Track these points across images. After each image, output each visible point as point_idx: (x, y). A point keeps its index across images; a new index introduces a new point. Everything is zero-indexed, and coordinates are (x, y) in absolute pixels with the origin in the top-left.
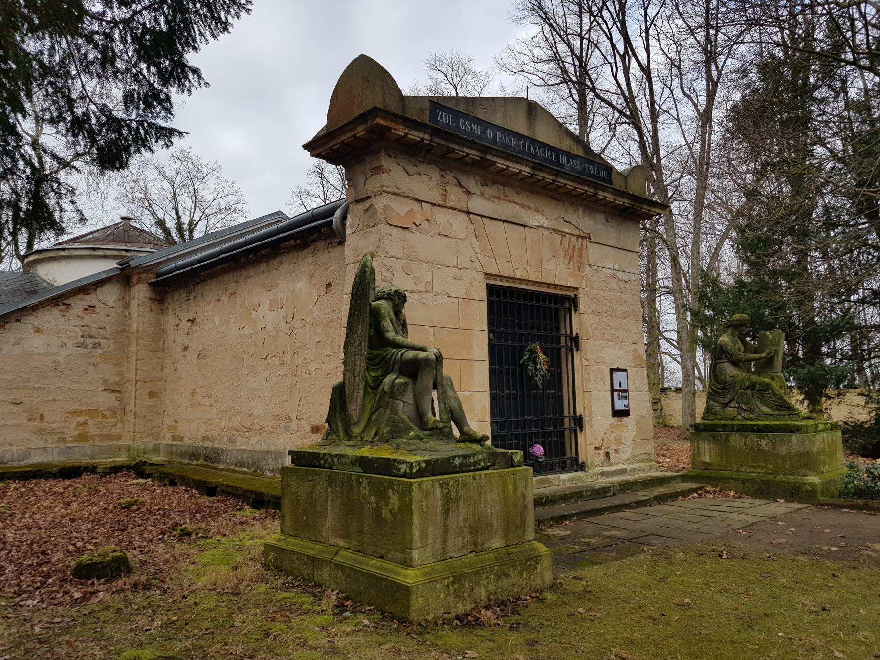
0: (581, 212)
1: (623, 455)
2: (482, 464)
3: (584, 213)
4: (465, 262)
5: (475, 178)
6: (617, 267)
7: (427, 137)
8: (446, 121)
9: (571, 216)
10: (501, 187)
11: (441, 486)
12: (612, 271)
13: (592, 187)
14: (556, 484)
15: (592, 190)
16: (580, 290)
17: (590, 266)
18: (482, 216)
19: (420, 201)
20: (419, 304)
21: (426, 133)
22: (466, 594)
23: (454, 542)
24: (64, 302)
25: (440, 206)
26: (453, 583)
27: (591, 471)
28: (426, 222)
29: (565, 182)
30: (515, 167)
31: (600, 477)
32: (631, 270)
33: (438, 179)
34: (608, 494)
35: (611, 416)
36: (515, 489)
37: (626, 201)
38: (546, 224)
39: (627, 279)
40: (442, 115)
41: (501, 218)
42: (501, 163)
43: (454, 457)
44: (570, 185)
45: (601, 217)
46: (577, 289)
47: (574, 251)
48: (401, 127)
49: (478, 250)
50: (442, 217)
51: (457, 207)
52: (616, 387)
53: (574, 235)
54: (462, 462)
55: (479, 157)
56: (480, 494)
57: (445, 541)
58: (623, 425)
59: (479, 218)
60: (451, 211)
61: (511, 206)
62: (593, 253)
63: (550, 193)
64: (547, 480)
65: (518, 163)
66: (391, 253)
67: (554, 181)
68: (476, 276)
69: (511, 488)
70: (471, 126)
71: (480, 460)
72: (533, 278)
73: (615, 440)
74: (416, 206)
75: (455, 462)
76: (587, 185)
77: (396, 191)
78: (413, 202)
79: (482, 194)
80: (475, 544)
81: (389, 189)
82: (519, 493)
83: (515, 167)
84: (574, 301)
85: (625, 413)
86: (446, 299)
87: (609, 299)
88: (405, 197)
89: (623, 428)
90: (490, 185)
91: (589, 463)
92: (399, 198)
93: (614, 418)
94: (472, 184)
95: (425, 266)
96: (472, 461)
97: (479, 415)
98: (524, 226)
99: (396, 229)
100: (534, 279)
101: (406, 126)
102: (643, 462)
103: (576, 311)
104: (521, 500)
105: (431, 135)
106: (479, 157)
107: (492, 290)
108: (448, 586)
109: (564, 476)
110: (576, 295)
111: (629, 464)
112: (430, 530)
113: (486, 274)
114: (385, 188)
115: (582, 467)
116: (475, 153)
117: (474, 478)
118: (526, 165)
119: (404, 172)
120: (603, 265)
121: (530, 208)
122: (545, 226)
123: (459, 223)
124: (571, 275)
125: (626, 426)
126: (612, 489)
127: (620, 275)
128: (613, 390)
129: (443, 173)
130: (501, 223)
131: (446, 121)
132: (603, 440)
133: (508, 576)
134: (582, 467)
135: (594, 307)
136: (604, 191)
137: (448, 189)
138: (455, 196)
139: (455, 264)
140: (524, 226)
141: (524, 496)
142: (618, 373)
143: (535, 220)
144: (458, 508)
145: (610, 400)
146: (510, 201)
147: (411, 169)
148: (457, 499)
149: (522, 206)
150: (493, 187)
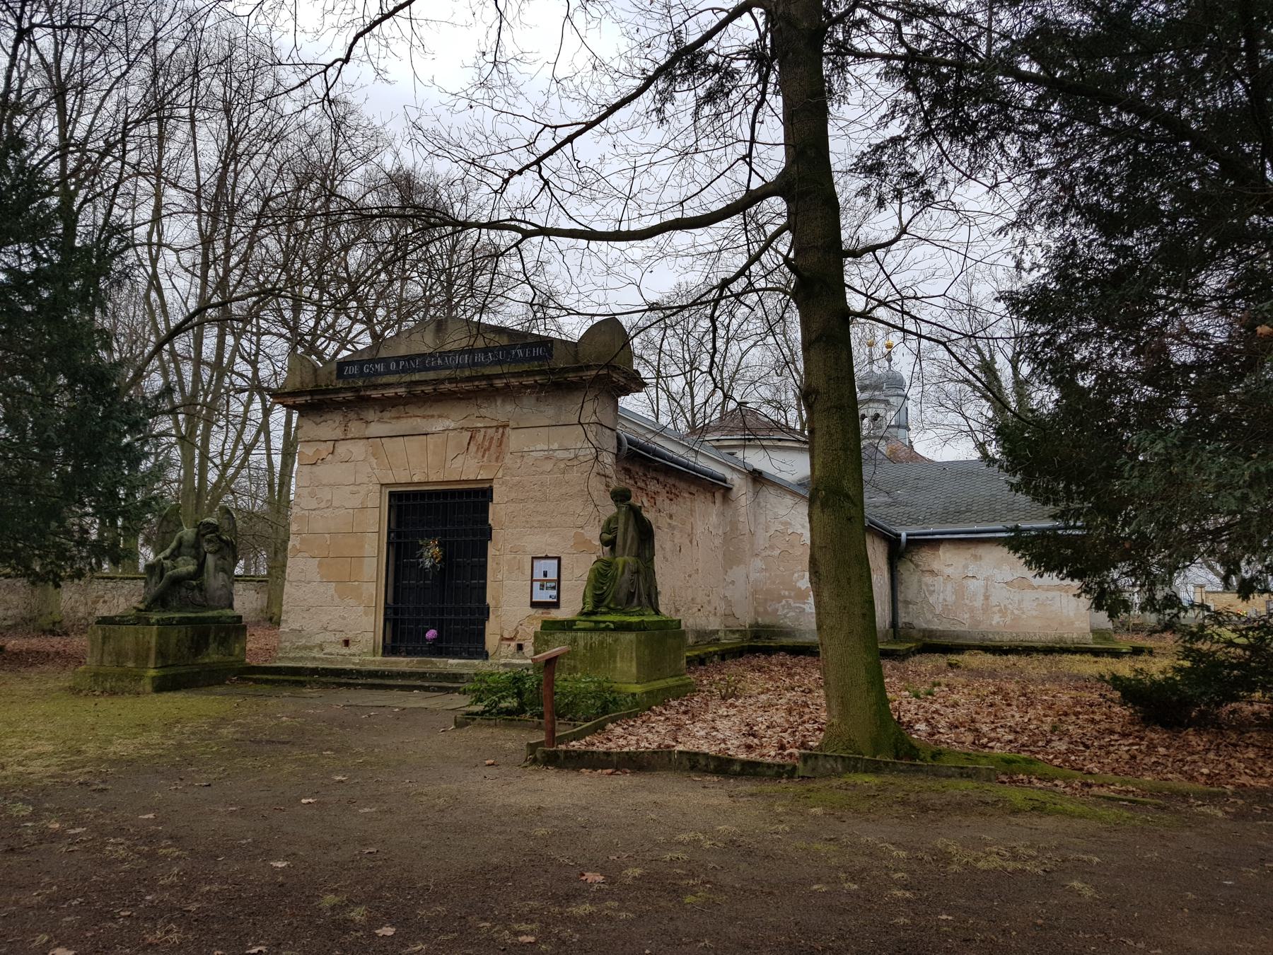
3: (503, 401)
6: (556, 446)
7: (308, 398)
23: (107, 659)
27: (490, 661)
37: (537, 378)
38: (452, 425)
45: (528, 401)
49: (375, 466)
50: (342, 448)
52: (538, 575)
61: (410, 420)
64: (432, 662)
72: (433, 478)
74: (322, 446)
86: (343, 511)
91: (490, 653)
94: (371, 415)
95: (327, 489)
107: (391, 494)
109: (451, 661)
116: (349, 394)
121: (432, 416)
123: (357, 450)
127: (560, 454)
128: (532, 581)
132: (517, 632)
134: (484, 655)
135: (513, 495)
138: (355, 428)
142: (543, 561)
143: (439, 425)
147: (318, 420)
148: (109, 637)
149: (424, 417)
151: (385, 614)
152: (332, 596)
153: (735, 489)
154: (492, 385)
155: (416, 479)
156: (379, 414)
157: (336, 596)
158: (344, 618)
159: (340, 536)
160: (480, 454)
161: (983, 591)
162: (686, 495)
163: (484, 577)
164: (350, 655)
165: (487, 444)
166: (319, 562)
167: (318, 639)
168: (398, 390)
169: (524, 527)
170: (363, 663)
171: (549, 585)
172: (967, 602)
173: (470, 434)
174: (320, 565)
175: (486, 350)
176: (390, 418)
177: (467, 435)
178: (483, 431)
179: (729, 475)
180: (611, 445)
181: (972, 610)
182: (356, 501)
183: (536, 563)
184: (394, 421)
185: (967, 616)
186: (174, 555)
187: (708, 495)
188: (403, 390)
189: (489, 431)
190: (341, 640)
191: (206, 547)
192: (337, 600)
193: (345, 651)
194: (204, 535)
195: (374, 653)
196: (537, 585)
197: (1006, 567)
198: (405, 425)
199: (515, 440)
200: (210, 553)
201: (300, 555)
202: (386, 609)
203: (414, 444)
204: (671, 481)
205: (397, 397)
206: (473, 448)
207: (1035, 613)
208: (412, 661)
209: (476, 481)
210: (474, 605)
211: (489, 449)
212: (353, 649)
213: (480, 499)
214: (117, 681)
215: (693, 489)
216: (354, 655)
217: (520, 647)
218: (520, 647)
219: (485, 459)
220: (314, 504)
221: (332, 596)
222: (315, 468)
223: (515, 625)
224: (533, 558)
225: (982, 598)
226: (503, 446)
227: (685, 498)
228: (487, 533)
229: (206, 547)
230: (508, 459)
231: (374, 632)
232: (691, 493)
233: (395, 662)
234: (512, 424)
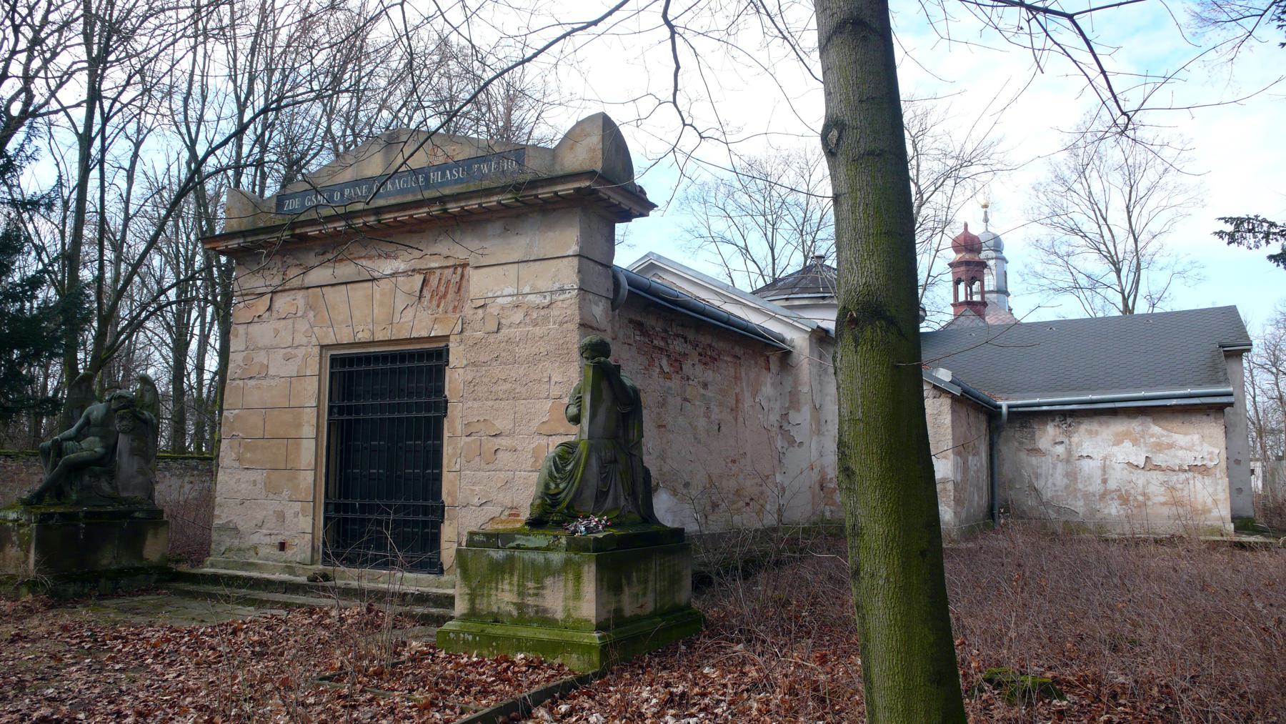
4: (300, 339)
6: (527, 290)
7: (241, 241)
16: (451, 337)
18: (321, 286)
29: (392, 215)
39: (547, 301)
46: (448, 336)
50: (282, 302)
53: (447, 267)
59: (319, 289)
72: (380, 336)
94: (312, 259)
100: (381, 339)
107: (334, 360)
110: (447, 346)
120: (498, 293)
130: (344, 287)
143: (387, 267)
151: (326, 510)
153: (795, 352)
154: (445, 211)
159: (276, 412)
160: (435, 303)
161: (1099, 472)
162: (728, 359)
163: (438, 464)
165: (442, 289)
167: (255, 539)
172: (1080, 486)
173: (422, 277)
177: (419, 279)
179: (788, 334)
180: (605, 286)
181: (1086, 496)
182: (291, 369)
185: (1081, 503)
186: (79, 436)
187: (761, 361)
190: (277, 543)
191: (117, 425)
194: (116, 411)
197: (1127, 444)
198: (346, 270)
199: (479, 282)
200: (123, 432)
202: (326, 505)
203: (360, 291)
204: (705, 340)
205: (337, 233)
206: (427, 293)
207: (1162, 499)
209: (429, 339)
210: (430, 503)
211: (445, 295)
212: (289, 554)
213: (434, 363)
215: (738, 350)
219: (440, 309)
225: (1099, 481)
226: (462, 292)
227: (726, 362)
228: (442, 406)
229: (117, 425)
231: (313, 533)
232: (736, 357)
234: (472, 262)
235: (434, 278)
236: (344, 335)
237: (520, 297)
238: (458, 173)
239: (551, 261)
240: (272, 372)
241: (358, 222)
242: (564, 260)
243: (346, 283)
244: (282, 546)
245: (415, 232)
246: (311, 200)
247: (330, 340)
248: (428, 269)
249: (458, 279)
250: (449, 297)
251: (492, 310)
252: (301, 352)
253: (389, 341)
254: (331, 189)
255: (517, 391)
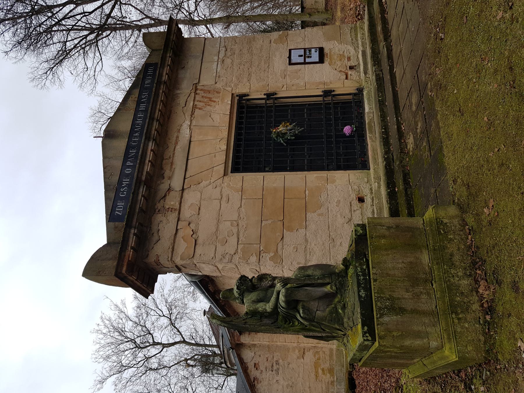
0: (178, 92)
1: (352, 53)
2: (364, 267)
3: (178, 89)
5: (159, 185)
7: (132, 231)
8: (121, 208)
9: (182, 100)
10: (164, 162)
11: (382, 315)
12: (219, 63)
13: (160, 86)
14: (372, 115)
15: (162, 87)
16: (233, 92)
17: (216, 83)
18: (185, 179)
19: (177, 230)
20: (246, 232)
21: (130, 232)
22: (466, 300)
24: (252, 381)
25: (179, 214)
26: (457, 314)
27: (364, 84)
28: (191, 225)
29: (157, 111)
30: (150, 155)
31: (367, 76)
32: (218, 46)
33: (161, 215)
34: (381, 76)
35: (324, 64)
36: (384, 237)
37: (168, 55)
38: (188, 122)
39: (224, 49)
40: (118, 211)
41: (185, 163)
42: (147, 167)
43: (360, 297)
44: (159, 106)
45: (181, 74)
46: (233, 94)
47: (206, 97)
48: (127, 253)
49: (208, 182)
50: (187, 213)
51: (179, 199)
52: (301, 60)
53: (195, 98)
54: (363, 288)
55: (144, 187)
56: (388, 275)
57: (424, 313)
58: (330, 53)
59: (186, 180)
60: (182, 204)
62: (207, 81)
63: (166, 119)
64: (369, 123)
65: (146, 153)
66: (213, 255)
67: (157, 120)
68: (226, 184)
69: (383, 241)
70: (124, 187)
71: (361, 269)
72: (225, 134)
73: (341, 60)
74: (180, 234)
75: (363, 296)
76: (159, 91)
77: (171, 250)
78: (178, 235)
79: (170, 178)
80: (426, 281)
81: (170, 256)
82: (387, 233)
83: (150, 155)
84: (241, 96)
85: (321, 51)
86: (243, 209)
87: (239, 66)
88: (174, 242)
89: (332, 53)
90: (163, 172)
91: (357, 85)
92: (175, 247)
93: (325, 61)
94: (164, 187)
95: (221, 227)
96: (362, 278)
97: (323, 182)
98: (190, 141)
99: (196, 250)
100: (227, 133)
101: (126, 248)
102: (357, 34)
103: (248, 95)
104: (392, 230)
105: (131, 227)
106: (144, 187)
107: (235, 170)
108: (459, 319)
110: (237, 96)
111: (358, 47)
112: (416, 328)
113: (224, 175)
114: (169, 259)
115: (360, 91)
116: (141, 190)
117: (375, 280)
118: (148, 145)
119: (158, 244)
120: (215, 71)
121: (177, 137)
122: (189, 124)
124: (223, 100)
125: (330, 49)
126: (377, 73)
127: (222, 55)
128: (305, 63)
129: (157, 211)
130: (189, 161)
131: (121, 208)
132: (341, 71)
133: (452, 255)
134: (360, 91)
135: (245, 80)
136: (162, 76)
137: (167, 207)
138: (172, 201)
139: (218, 201)
140: (190, 141)
141: (389, 228)
142: (292, 58)
143: (185, 132)
144: (399, 299)
145: (312, 65)
146: (174, 154)
147: (155, 238)
148: (391, 299)
149: (176, 143)
150: (165, 168)
152: (319, 215)
155: (224, 147)
156: (166, 178)
157: (319, 212)
158: (339, 202)
159: (265, 210)
160: (213, 104)
164: (372, 193)
165: (206, 100)
166: (288, 230)
168: (150, 148)
169: (268, 72)
170: (378, 179)
171: (308, 53)
174: (290, 229)
175: (139, 103)
176: (171, 170)
178: (196, 103)
183: (293, 61)
184: (173, 167)
188: (150, 144)
189: (197, 99)
190: (359, 205)
192: (323, 210)
193: (368, 200)
195: (369, 174)
196: (308, 60)
201: (280, 252)
208: (371, 138)
212: (366, 193)
214: (452, 265)
216: (371, 189)
217: (351, 68)
218: (351, 68)
219: (217, 100)
220: (233, 240)
221: (319, 215)
222: (200, 241)
223: (335, 72)
224: (290, 64)
230: (219, 85)
233: (374, 150)
235: (200, 105)
236: (221, 158)
237: (219, 60)
238: (144, 95)
239: (205, 48)
240: (235, 217)
241: (153, 133)
242: (206, 43)
243: (187, 160)
244: (361, 200)
245: (170, 115)
246: (124, 191)
247: (221, 168)
248: (193, 108)
249: (202, 92)
250: (210, 96)
251: (223, 73)
252: (226, 191)
253: (230, 115)
254: (122, 175)
255: (265, 58)
